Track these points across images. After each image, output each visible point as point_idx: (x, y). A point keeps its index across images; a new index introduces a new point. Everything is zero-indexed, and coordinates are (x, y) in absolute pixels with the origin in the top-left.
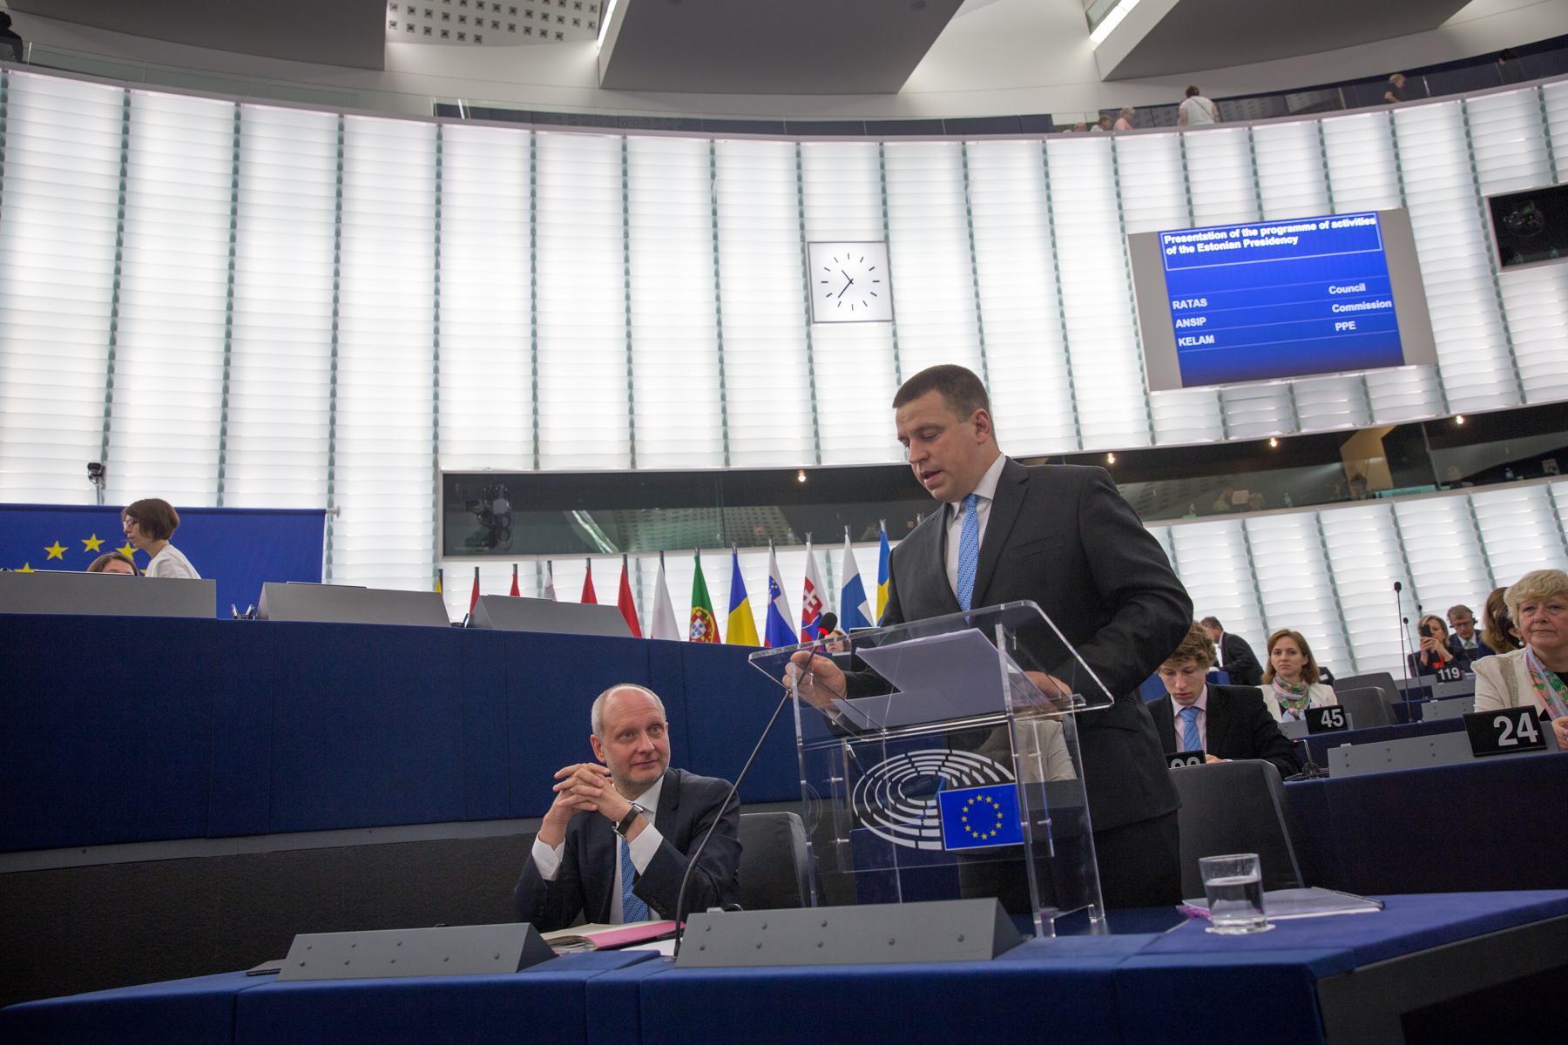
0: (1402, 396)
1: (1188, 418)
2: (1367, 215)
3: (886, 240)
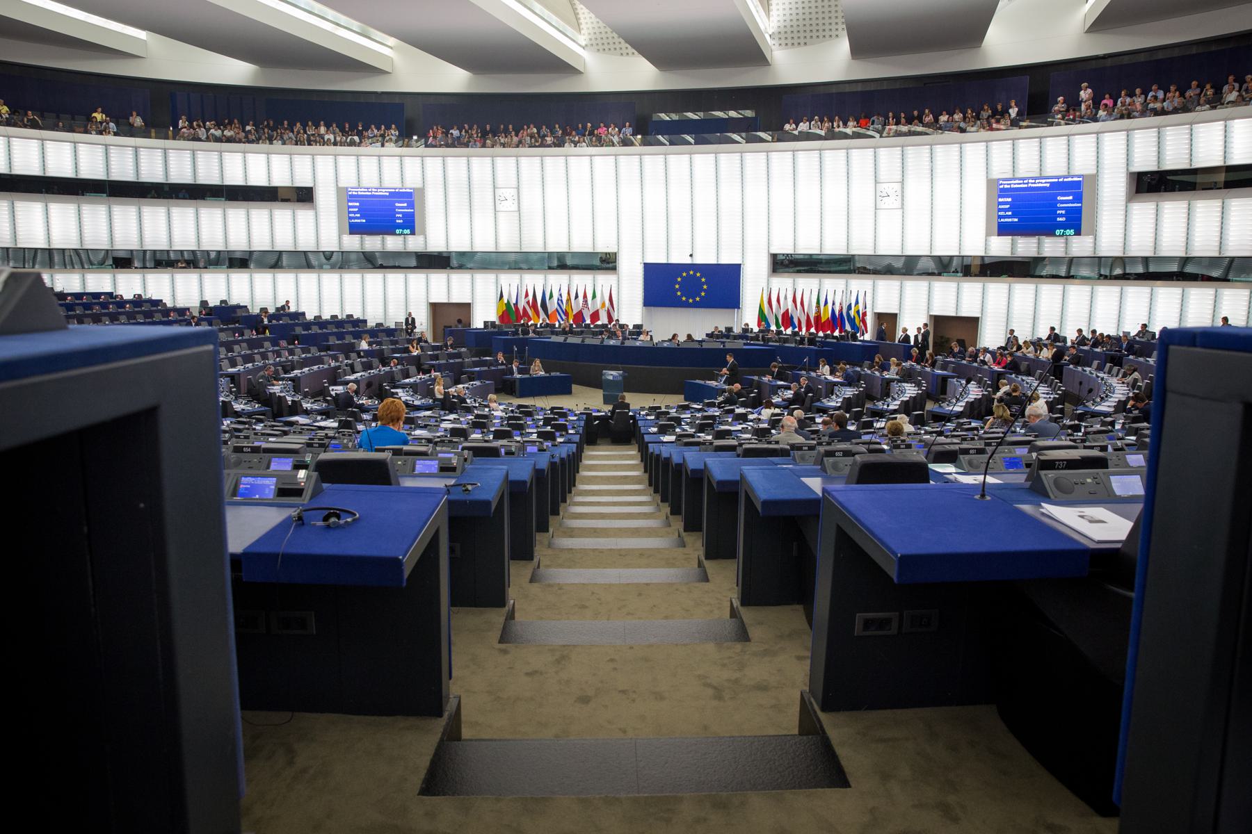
0: (1080, 246)
1: (1001, 247)
2: (1079, 176)
3: (902, 182)
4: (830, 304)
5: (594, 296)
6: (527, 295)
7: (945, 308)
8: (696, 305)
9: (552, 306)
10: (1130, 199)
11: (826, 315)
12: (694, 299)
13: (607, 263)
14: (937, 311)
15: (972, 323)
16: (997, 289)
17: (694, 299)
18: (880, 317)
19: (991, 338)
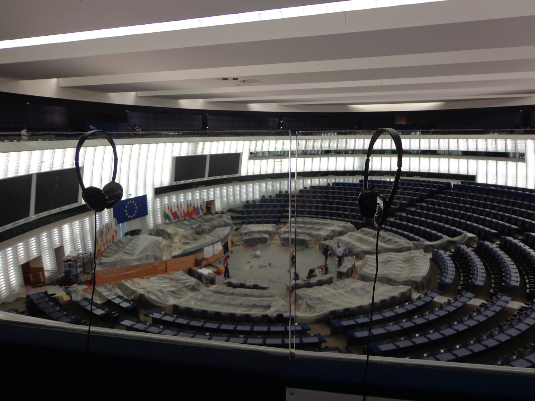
8: (134, 218)
11: (191, 209)
19: (218, 206)
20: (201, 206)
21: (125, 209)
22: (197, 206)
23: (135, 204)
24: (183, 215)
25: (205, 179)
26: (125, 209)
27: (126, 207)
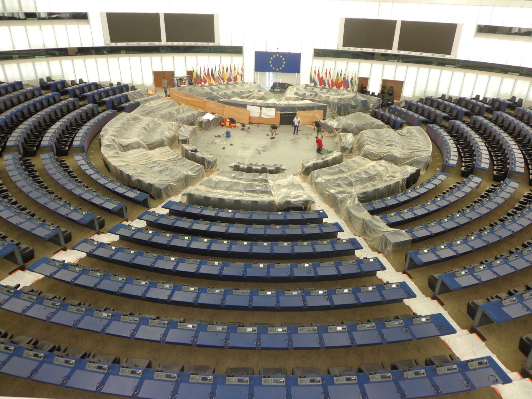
4: (343, 76)
5: (235, 69)
6: (204, 70)
7: (389, 77)
8: (279, 71)
9: (216, 74)
10: (475, 36)
11: (341, 79)
12: (279, 68)
13: (237, 50)
14: (386, 78)
15: (400, 84)
16: (413, 69)
17: (279, 68)
18: (361, 79)
20: (352, 79)
21: (270, 60)
22: (348, 79)
23: (284, 59)
24: (330, 83)
25: (394, 50)
26: (270, 60)
27: (272, 59)
